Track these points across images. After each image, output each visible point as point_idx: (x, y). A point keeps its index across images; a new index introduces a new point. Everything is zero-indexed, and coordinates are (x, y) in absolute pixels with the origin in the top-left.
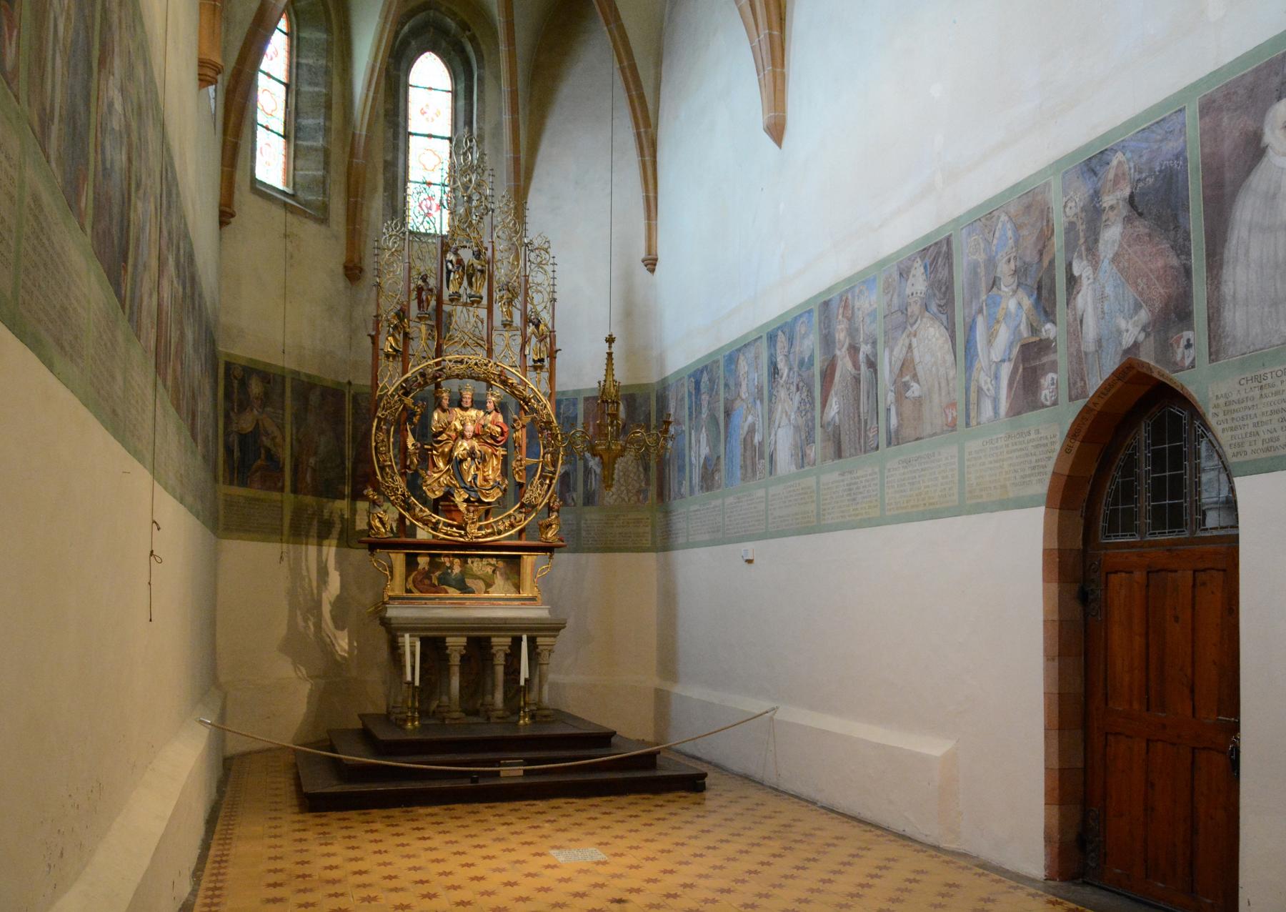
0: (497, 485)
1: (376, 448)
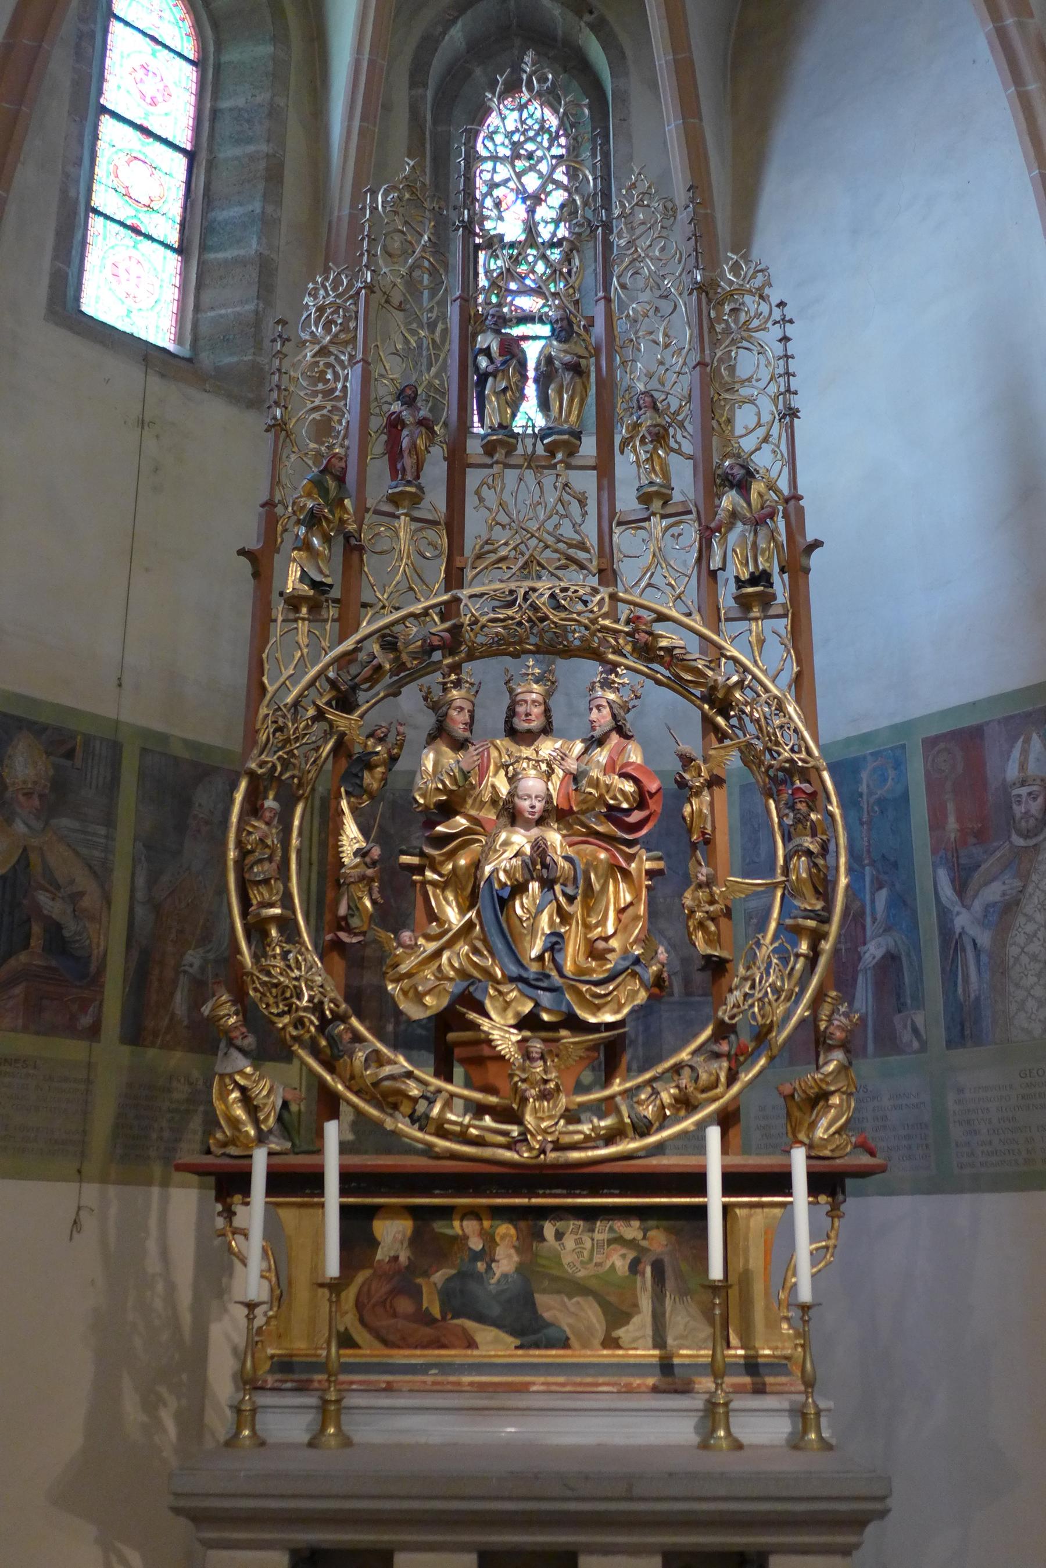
1: (239, 864)
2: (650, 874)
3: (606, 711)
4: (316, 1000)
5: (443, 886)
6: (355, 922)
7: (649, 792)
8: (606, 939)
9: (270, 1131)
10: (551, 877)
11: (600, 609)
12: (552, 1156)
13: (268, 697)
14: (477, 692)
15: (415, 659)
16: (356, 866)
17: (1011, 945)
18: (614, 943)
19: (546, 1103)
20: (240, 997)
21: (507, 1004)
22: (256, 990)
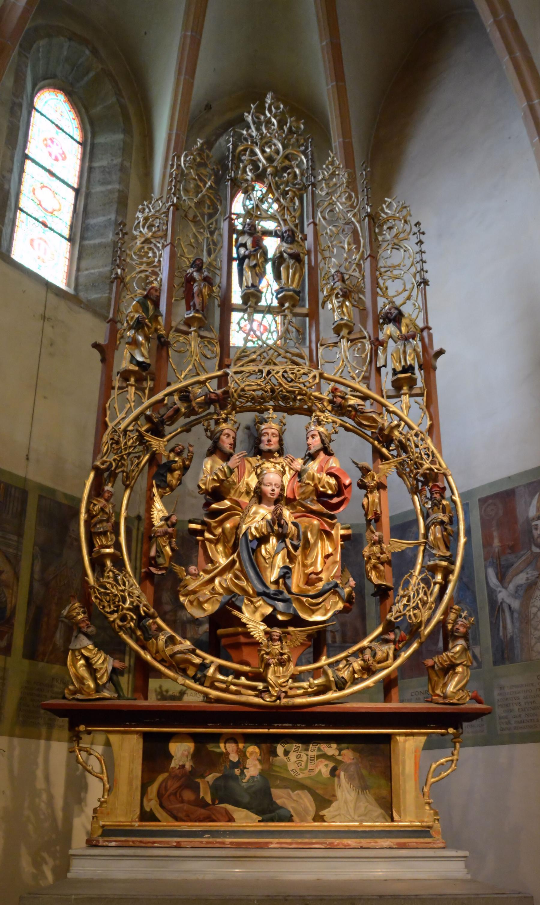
0: (334, 589)
2: (343, 537)
3: (318, 438)
4: (135, 604)
5: (216, 542)
6: (160, 560)
7: (344, 484)
8: (317, 574)
9: (104, 685)
10: (284, 532)
11: (313, 381)
12: (284, 701)
13: (109, 429)
14: (238, 428)
15: (200, 407)
16: (161, 526)
17: (532, 607)
18: (323, 576)
19: (281, 668)
20: (87, 604)
21: (256, 609)
22: (96, 597)
